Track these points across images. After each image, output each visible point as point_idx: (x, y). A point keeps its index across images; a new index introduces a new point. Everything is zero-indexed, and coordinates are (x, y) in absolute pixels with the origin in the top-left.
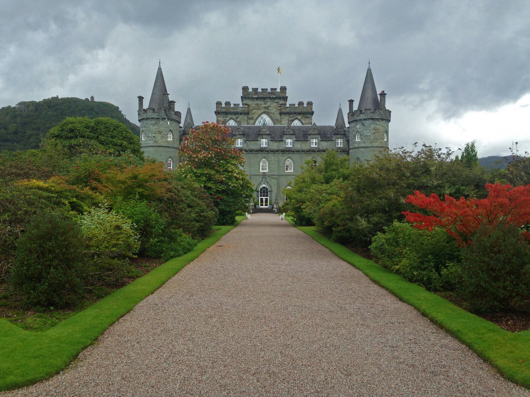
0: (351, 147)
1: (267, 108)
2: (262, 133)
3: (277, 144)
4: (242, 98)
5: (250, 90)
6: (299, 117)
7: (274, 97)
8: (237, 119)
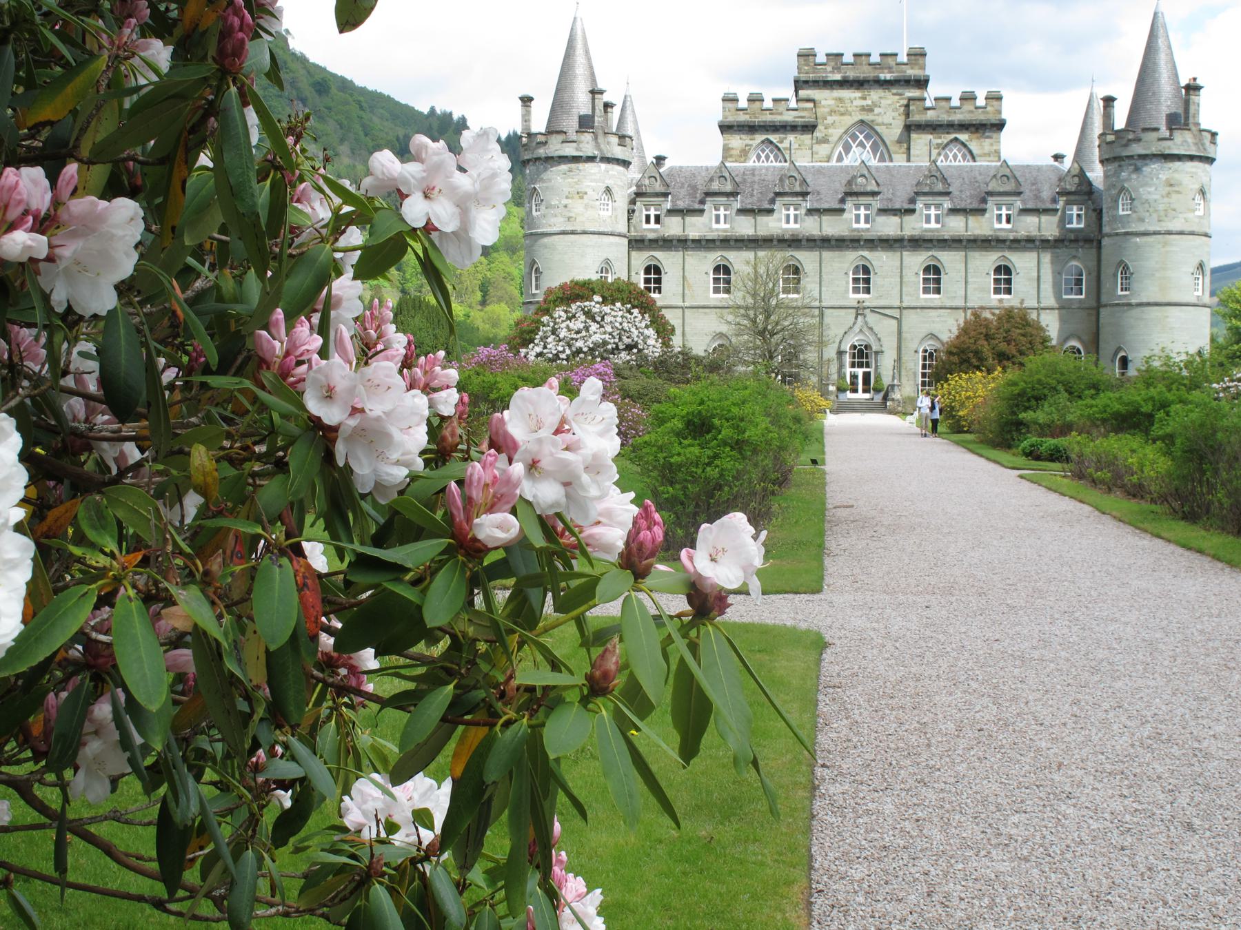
0: (1106, 229)
1: (870, 110)
2: (855, 189)
3: (895, 220)
4: (796, 82)
5: (821, 58)
6: (963, 137)
7: (889, 76)
8: (781, 142)
